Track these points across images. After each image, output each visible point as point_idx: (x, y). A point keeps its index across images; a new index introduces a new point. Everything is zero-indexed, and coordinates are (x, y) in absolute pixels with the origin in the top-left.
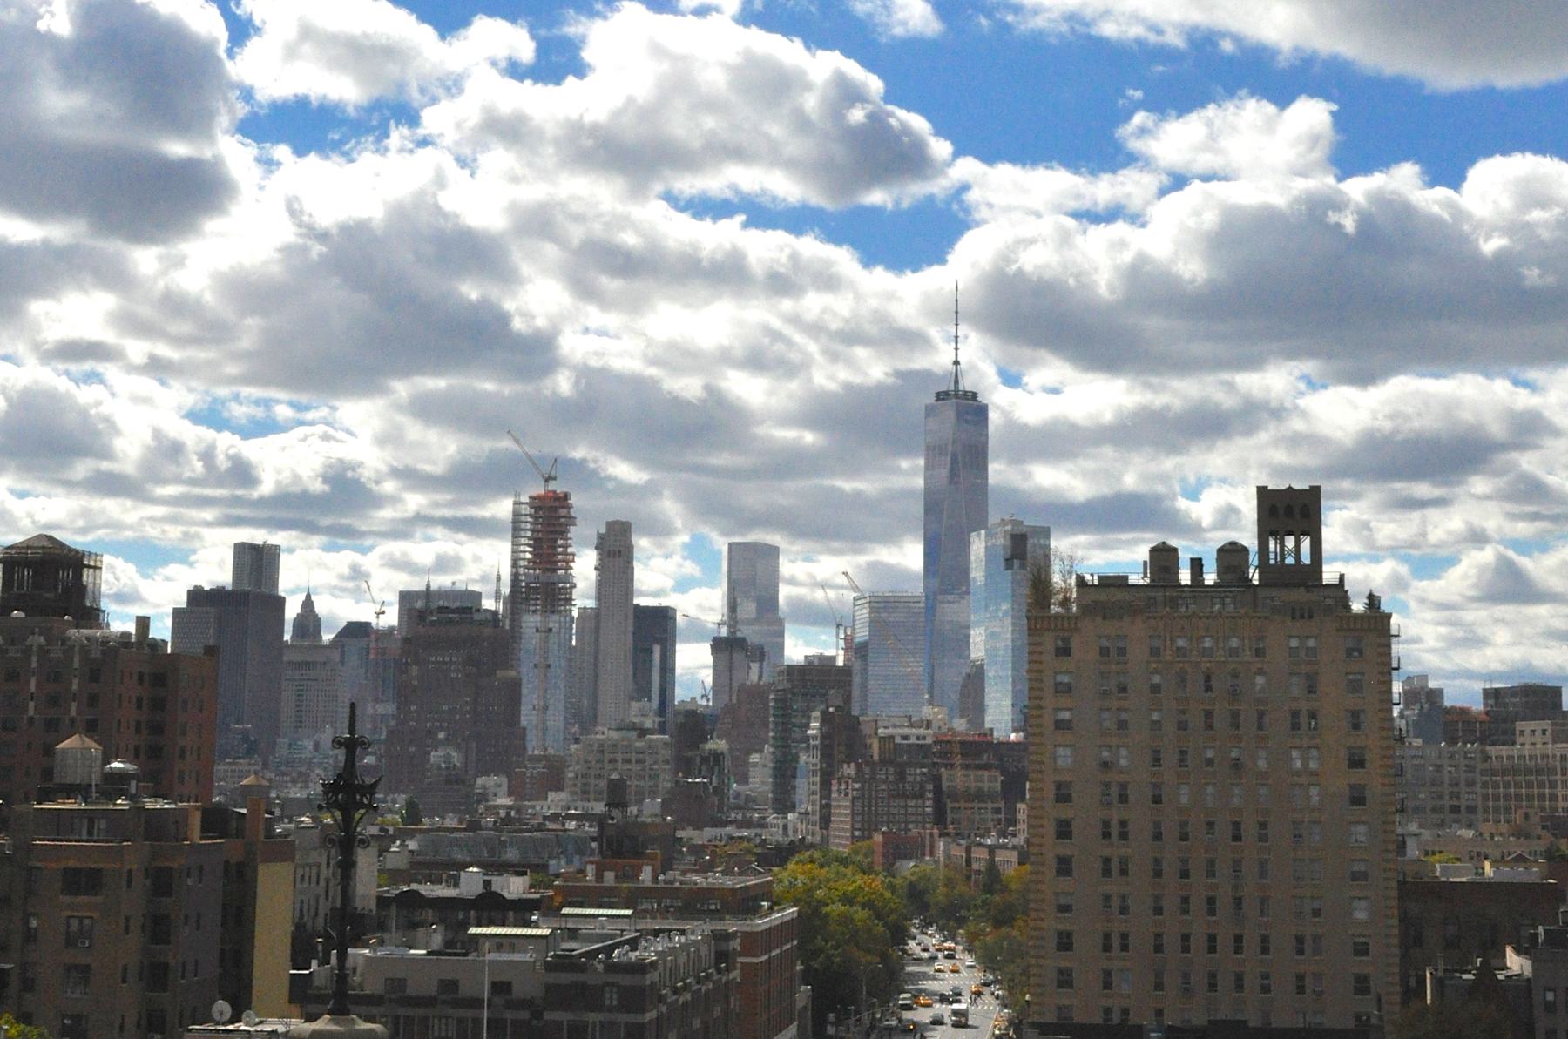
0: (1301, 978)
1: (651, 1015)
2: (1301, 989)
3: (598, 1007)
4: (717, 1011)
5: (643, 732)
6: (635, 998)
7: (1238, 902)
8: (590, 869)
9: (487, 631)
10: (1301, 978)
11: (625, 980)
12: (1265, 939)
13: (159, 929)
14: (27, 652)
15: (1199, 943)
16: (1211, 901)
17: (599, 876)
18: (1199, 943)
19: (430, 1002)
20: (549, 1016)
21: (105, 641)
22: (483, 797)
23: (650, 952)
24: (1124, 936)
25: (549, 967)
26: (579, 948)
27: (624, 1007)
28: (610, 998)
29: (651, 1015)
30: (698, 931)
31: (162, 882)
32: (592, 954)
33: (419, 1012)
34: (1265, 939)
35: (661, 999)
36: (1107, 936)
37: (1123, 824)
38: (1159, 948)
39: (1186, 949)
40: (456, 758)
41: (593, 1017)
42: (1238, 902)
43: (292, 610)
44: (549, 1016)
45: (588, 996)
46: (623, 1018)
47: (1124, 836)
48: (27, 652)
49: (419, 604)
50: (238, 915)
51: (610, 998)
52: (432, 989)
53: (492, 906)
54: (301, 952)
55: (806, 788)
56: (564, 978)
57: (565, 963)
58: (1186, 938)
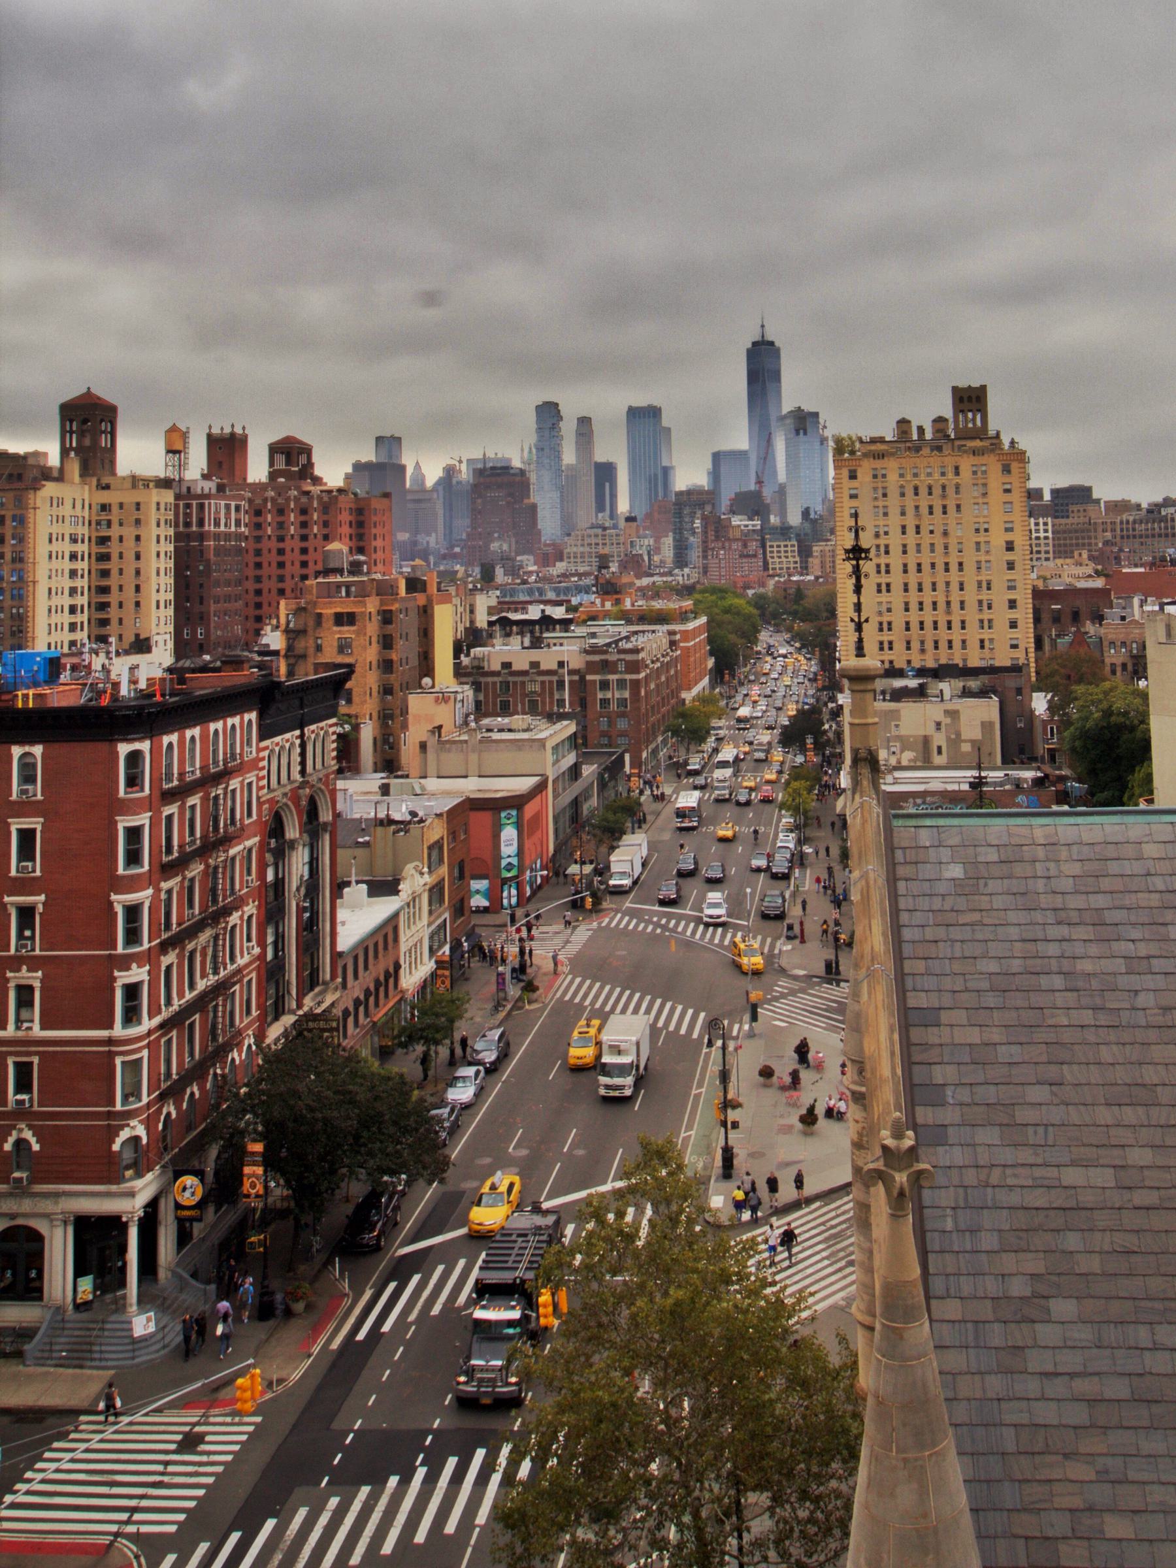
0: (982, 641)
1: (642, 675)
2: (982, 647)
3: (615, 672)
4: (672, 672)
5: (605, 529)
6: (634, 667)
7: (948, 603)
8: (598, 601)
9: (518, 479)
10: (982, 641)
11: (629, 657)
12: (963, 622)
13: (387, 642)
14: (288, 499)
15: (928, 625)
16: (935, 603)
17: (603, 605)
18: (928, 625)
19: (524, 673)
20: (589, 677)
21: (330, 492)
22: (521, 567)
23: (639, 641)
24: (890, 623)
25: (586, 652)
26: (600, 641)
27: (628, 671)
28: (621, 667)
29: (642, 675)
30: (662, 629)
31: (387, 618)
32: (609, 645)
33: (520, 679)
34: (963, 622)
35: (647, 666)
36: (881, 624)
37: (887, 566)
38: (908, 629)
39: (922, 629)
40: (505, 547)
41: (612, 677)
42: (948, 603)
43: (409, 471)
44: (589, 677)
45: (606, 666)
46: (628, 677)
47: (888, 572)
48: (288, 499)
49: (480, 466)
50: (426, 634)
51: (621, 667)
52: (526, 667)
53: (547, 622)
54: (458, 650)
55: (695, 555)
56: (597, 658)
57: (594, 650)
58: (922, 623)
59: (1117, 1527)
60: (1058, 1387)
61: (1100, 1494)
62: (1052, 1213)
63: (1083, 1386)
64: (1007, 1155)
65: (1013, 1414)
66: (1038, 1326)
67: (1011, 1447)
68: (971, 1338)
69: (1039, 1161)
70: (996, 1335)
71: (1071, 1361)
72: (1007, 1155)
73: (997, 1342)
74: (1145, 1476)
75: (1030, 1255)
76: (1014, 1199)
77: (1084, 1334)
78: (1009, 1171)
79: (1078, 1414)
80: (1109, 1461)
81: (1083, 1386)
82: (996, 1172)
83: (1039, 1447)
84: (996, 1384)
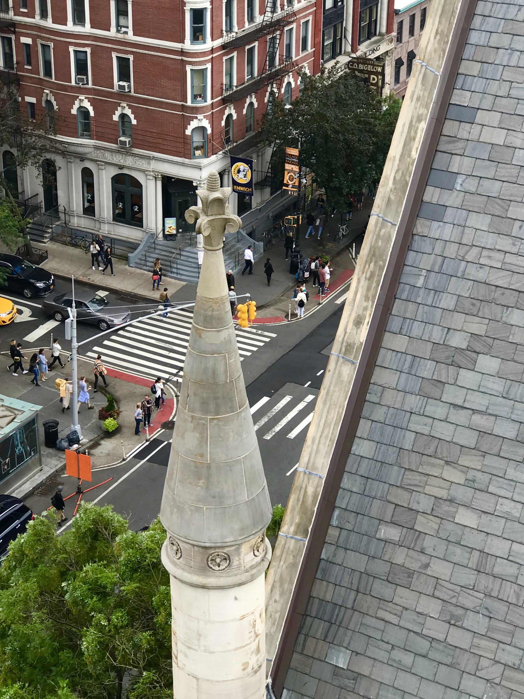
59: (465, 517)
60: (461, 417)
61: (462, 494)
62: (507, 292)
63: (478, 420)
64: (489, 240)
65: (418, 424)
66: (462, 372)
67: (407, 445)
68: (407, 365)
69: (515, 250)
70: (427, 369)
71: (477, 401)
72: (489, 240)
73: (426, 374)
74: (502, 493)
75: (477, 319)
76: (481, 275)
77: (496, 386)
78: (485, 253)
79: (468, 438)
80: (479, 475)
81: (478, 420)
82: (475, 251)
83: (430, 451)
84: (413, 402)
